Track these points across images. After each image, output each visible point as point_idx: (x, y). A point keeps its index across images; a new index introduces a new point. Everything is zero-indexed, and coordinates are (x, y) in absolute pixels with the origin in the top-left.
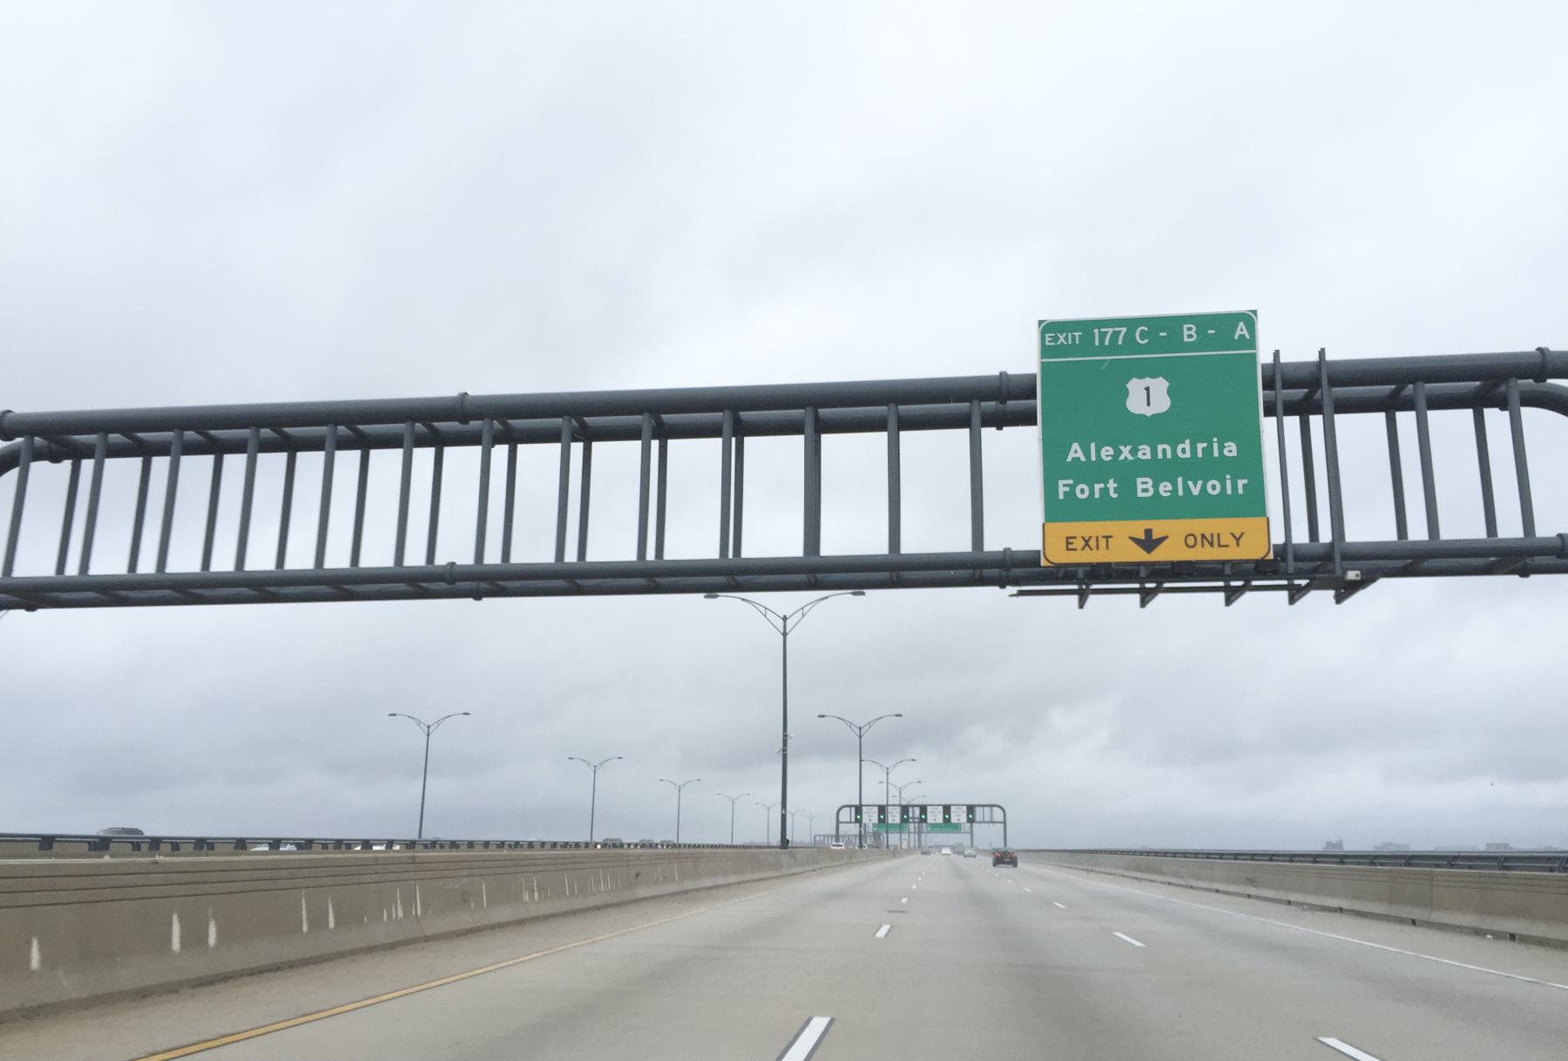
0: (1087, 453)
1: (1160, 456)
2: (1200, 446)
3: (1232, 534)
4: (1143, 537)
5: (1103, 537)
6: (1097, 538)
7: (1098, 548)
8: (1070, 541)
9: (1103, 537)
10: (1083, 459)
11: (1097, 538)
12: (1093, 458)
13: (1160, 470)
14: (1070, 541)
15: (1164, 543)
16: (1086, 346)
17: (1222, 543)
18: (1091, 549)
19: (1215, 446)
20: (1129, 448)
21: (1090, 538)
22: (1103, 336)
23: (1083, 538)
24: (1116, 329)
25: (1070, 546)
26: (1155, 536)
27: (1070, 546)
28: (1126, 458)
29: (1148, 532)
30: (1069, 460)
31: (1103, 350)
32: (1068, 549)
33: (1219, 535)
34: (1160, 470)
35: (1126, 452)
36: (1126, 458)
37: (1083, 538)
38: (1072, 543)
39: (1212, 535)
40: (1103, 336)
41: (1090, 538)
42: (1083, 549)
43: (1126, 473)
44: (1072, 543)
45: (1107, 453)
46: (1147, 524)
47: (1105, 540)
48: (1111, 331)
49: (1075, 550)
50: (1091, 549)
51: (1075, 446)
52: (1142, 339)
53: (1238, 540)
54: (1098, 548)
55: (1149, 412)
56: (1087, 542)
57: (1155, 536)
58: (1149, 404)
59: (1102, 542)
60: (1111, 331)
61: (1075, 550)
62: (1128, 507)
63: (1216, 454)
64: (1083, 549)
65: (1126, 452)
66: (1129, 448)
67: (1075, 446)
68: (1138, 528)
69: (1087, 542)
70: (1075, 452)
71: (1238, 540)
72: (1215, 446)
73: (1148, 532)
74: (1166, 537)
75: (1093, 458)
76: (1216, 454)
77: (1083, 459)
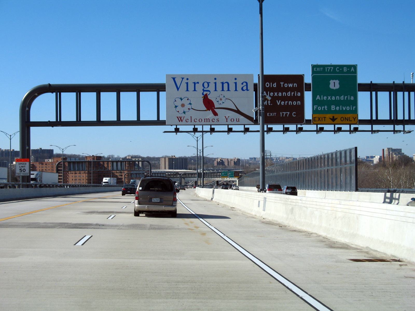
0: (320, 98)
1: (337, 99)
2: (346, 97)
3: (353, 117)
4: (332, 118)
5: (324, 117)
6: (322, 118)
7: (322, 121)
8: (315, 118)
9: (324, 117)
10: (320, 99)
11: (322, 118)
12: (322, 99)
13: (337, 103)
14: (315, 118)
15: (337, 120)
16: (324, 71)
17: (350, 120)
18: (320, 121)
19: (349, 97)
20: (330, 97)
21: (320, 118)
22: (328, 69)
23: (318, 118)
24: (331, 68)
25: (315, 120)
26: (335, 118)
27: (315, 120)
28: (329, 99)
29: (333, 117)
30: (317, 99)
31: (327, 73)
32: (314, 121)
33: (349, 118)
34: (337, 103)
35: (329, 98)
36: (329, 99)
37: (318, 118)
38: (315, 119)
39: (348, 118)
40: (328, 69)
41: (320, 118)
42: (318, 121)
43: (330, 103)
44: (315, 119)
45: (325, 98)
46: (334, 115)
47: (324, 118)
48: (329, 68)
49: (316, 121)
50: (320, 121)
51: (318, 96)
52: (338, 70)
53: (354, 119)
54: (322, 121)
55: (334, 88)
56: (319, 119)
57: (335, 118)
58: (334, 86)
59: (323, 119)
60: (329, 68)
61: (316, 121)
62: (329, 111)
63: (349, 99)
64: (318, 121)
65: (329, 98)
66: (330, 97)
67: (318, 96)
68: (330, 116)
69: (319, 119)
70: (318, 97)
71: (354, 119)
72: (349, 97)
73: (333, 117)
74: (337, 118)
75: (322, 99)
76: (349, 99)
77: (320, 99)
